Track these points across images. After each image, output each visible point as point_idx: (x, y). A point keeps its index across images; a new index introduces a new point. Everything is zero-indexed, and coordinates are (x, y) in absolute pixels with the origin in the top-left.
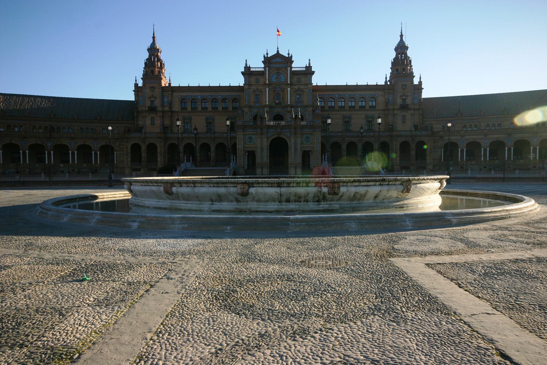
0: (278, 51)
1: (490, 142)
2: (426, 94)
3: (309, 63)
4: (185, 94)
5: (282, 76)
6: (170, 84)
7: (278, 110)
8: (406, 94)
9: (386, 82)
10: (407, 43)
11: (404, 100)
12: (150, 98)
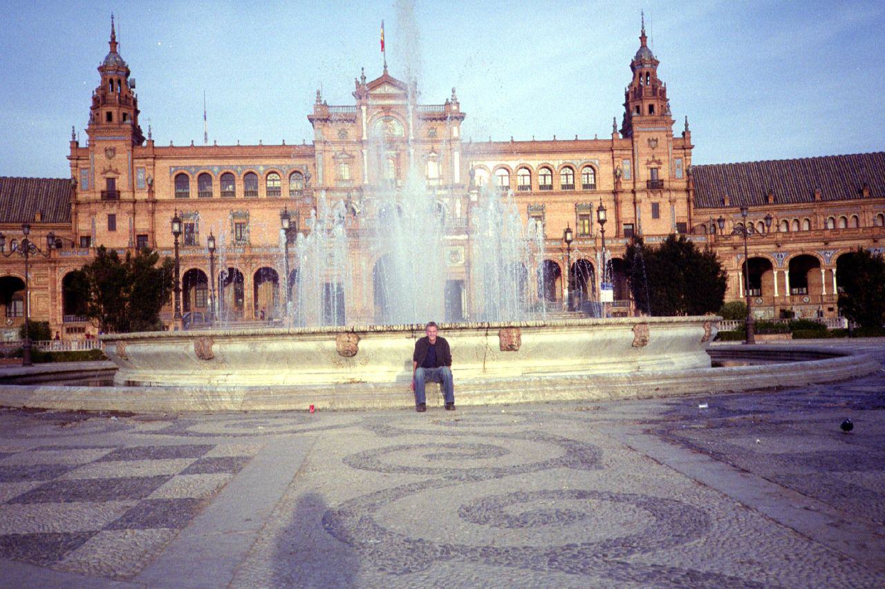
0: (385, 71)
1: (836, 256)
8: (657, 158)
9: (615, 131)
12: (105, 172)
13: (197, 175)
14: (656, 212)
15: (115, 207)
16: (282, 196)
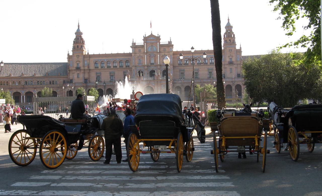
0: (152, 33)
2: (243, 54)
3: (170, 39)
4: (97, 59)
5: (154, 48)
6: (88, 53)
7: (152, 68)
8: (231, 55)
10: (232, 24)
12: (77, 62)
16: (124, 67)
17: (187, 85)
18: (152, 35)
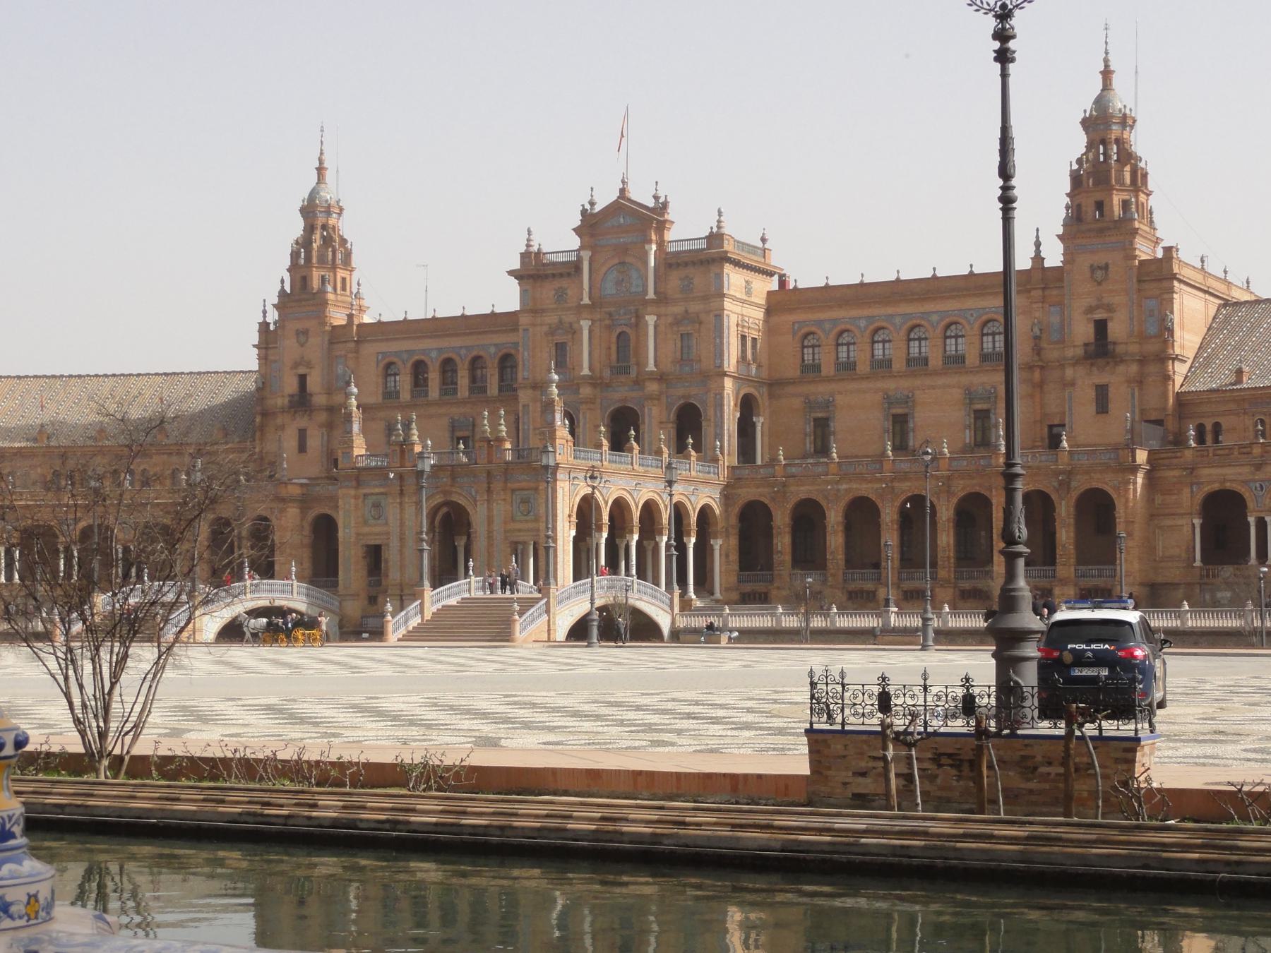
0: (622, 191)
7: (621, 394)
8: (1105, 301)
11: (1101, 326)
13: (409, 365)
14: (1102, 405)
15: (306, 418)
17: (803, 496)
18: (622, 206)
